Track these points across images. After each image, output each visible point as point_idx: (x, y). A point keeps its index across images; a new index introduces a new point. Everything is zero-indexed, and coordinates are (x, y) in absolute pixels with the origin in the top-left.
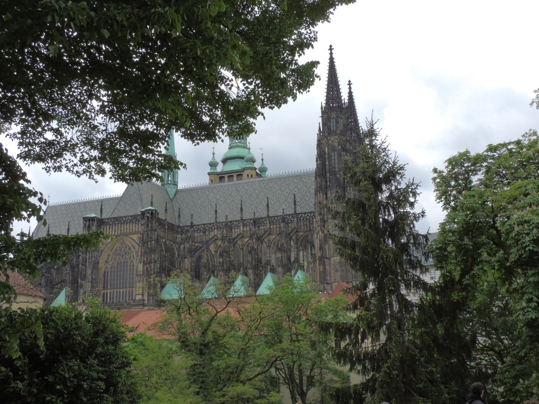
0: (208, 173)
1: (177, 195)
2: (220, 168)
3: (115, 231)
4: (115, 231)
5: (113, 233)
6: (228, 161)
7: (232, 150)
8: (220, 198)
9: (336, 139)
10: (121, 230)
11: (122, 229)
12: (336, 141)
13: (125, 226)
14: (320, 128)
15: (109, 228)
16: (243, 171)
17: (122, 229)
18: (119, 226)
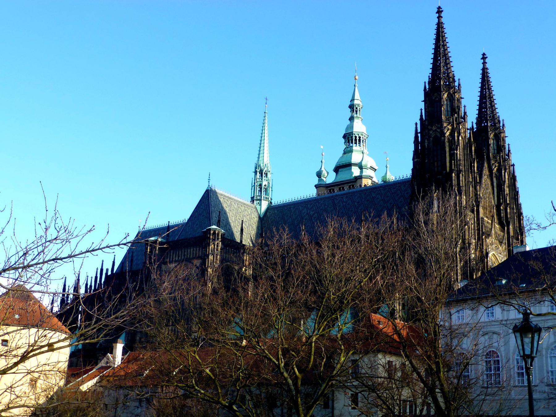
0: (315, 186)
1: (268, 214)
2: (330, 178)
3: (179, 257)
4: (179, 257)
5: (177, 259)
6: (340, 170)
7: (345, 155)
8: (314, 214)
9: (438, 128)
10: (184, 255)
11: (186, 253)
12: (439, 130)
13: (189, 250)
14: (421, 116)
15: (173, 253)
16: (355, 181)
17: (186, 253)
18: (183, 251)
